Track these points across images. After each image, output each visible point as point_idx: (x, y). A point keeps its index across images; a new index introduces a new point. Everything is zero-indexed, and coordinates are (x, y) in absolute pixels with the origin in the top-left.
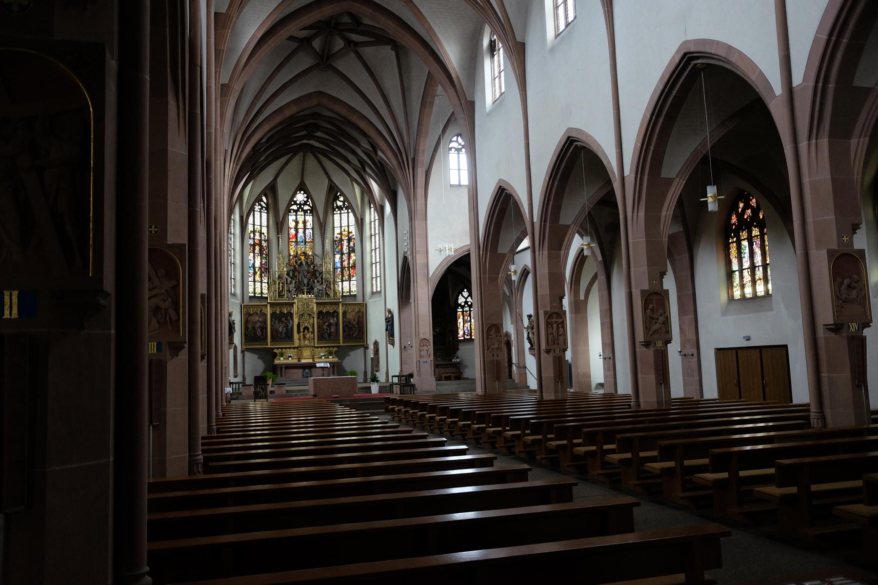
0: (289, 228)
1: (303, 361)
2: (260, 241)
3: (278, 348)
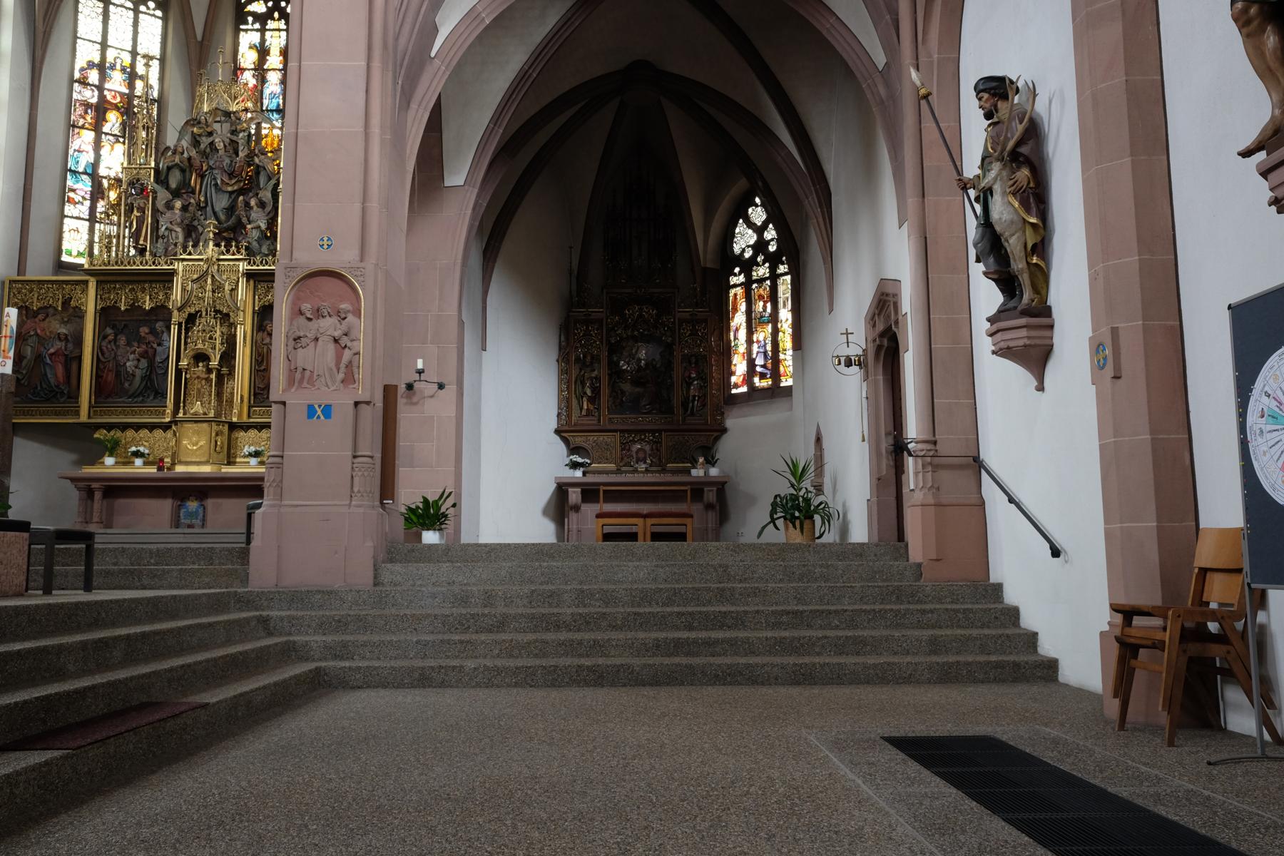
0: (237, 70)
1: (180, 469)
2: (129, 97)
3: (110, 427)
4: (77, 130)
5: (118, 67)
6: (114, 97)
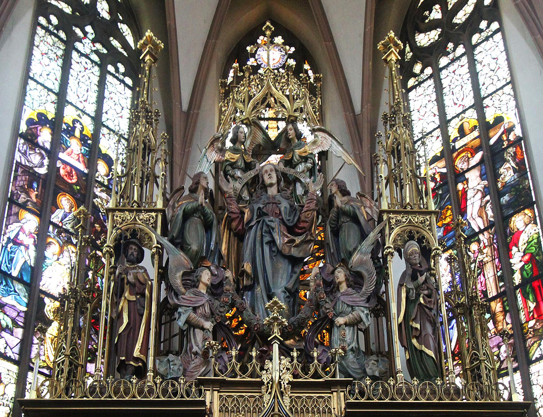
4: (15, 209)
5: (77, 133)
6: (70, 174)
